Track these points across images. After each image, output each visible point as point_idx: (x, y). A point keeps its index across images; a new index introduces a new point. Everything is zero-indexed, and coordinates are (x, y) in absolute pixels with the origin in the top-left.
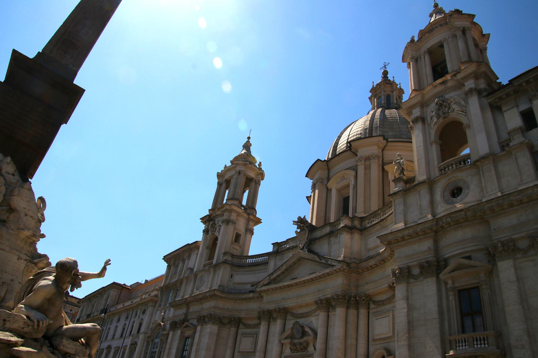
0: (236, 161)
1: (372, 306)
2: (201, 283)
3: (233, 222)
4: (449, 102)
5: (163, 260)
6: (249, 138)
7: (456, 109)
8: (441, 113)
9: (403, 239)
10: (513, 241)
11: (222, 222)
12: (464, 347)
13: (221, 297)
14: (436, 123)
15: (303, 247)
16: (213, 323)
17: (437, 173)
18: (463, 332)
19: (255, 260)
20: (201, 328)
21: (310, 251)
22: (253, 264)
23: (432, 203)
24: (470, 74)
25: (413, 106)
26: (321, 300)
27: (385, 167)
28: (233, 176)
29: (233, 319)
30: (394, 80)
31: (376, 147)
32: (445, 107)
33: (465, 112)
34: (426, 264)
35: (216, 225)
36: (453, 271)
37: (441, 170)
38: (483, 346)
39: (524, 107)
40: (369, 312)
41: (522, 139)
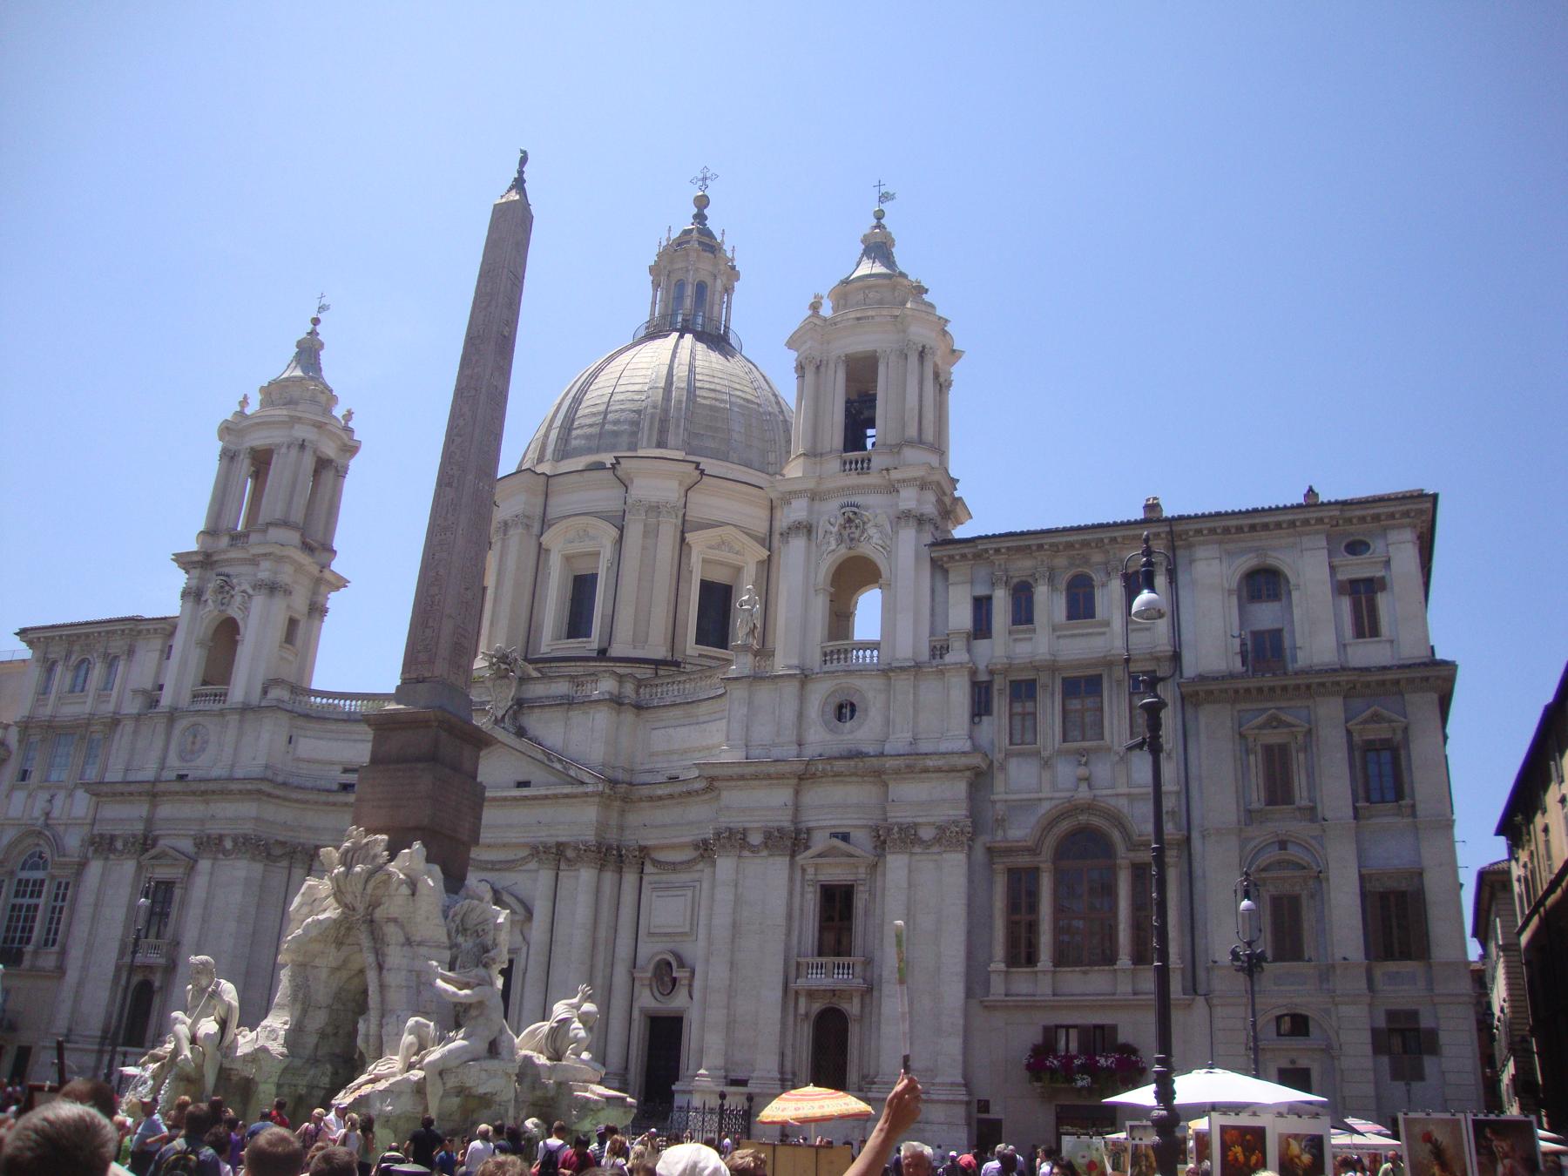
0: (276, 392)
1: (649, 868)
2: (193, 743)
3: (285, 591)
4: (865, 519)
5: (18, 638)
6: (316, 321)
7: (874, 540)
8: (845, 533)
9: (742, 777)
10: (916, 825)
11: (259, 586)
12: (819, 976)
13: (269, 795)
14: (833, 551)
15: (504, 716)
16: (253, 859)
17: (818, 657)
18: (820, 954)
19: (351, 706)
20: (213, 865)
21: (521, 732)
22: (345, 717)
23: (801, 715)
24: (915, 479)
25: (795, 492)
26: (547, 849)
27: (686, 535)
28: (280, 446)
29: (300, 848)
30: (722, 241)
31: (674, 484)
32: (857, 527)
33: (889, 551)
34: (776, 834)
35: (233, 588)
36: (819, 856)
37: (825, 655)
38: (846, 976)
39: (981, 591)
40: (641, 879)
41: (965, 657)
